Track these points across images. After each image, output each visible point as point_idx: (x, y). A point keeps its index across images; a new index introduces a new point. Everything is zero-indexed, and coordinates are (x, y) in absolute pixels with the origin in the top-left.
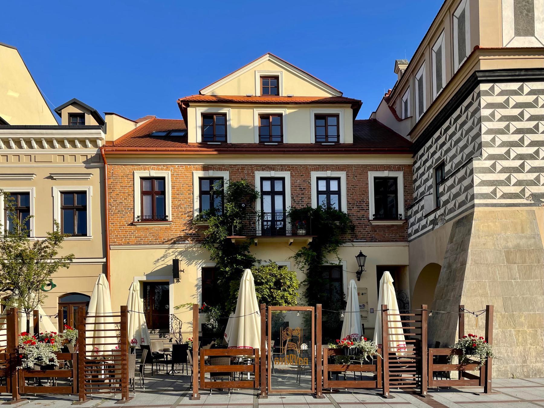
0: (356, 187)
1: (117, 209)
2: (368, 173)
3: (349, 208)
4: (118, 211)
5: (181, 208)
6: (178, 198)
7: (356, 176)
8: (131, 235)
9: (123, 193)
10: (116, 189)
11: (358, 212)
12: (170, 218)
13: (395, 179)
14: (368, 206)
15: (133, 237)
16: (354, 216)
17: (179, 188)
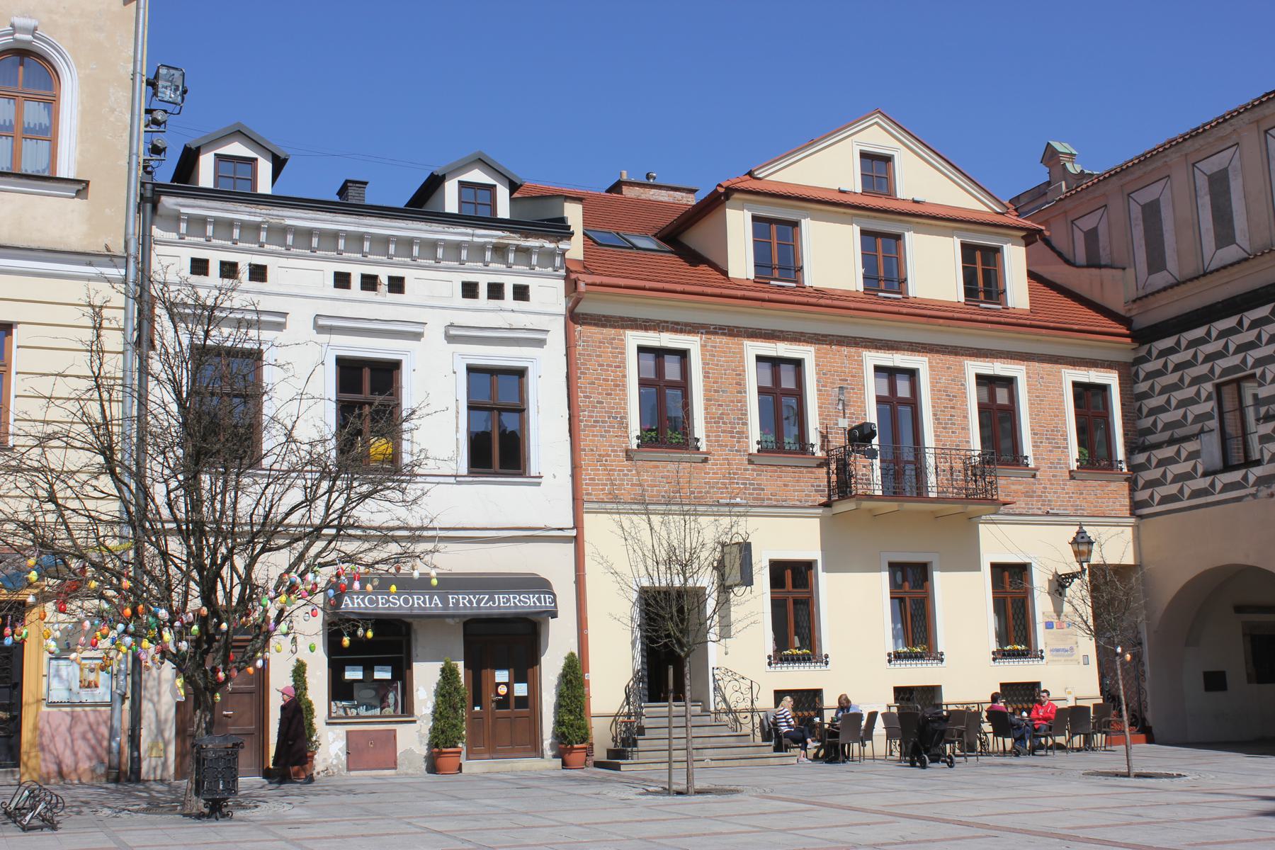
0: (1042, 401)
1: (592, 417)
2: (1061, 372)
3: (1035, 442)
4: (595, 422)
5: (724, 423)
6: (718, 401)
7: (1042, 378)
8: (623, 480)
9: (604, 380)
10: (588, 369)
11: (1051, 451)
12: (703, 446)
13: (1104, 389)
14: (1066, 439)
15: (627, 484)
16: (1044, 459)
17: (716, 378)
